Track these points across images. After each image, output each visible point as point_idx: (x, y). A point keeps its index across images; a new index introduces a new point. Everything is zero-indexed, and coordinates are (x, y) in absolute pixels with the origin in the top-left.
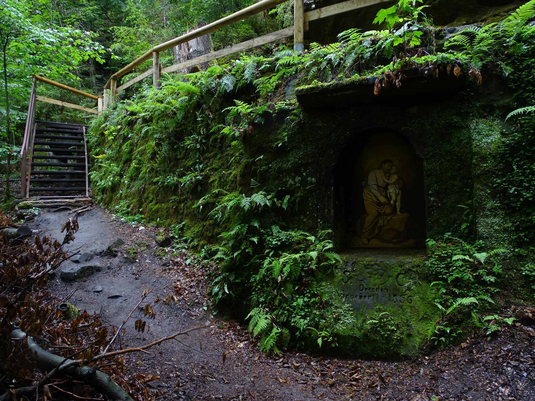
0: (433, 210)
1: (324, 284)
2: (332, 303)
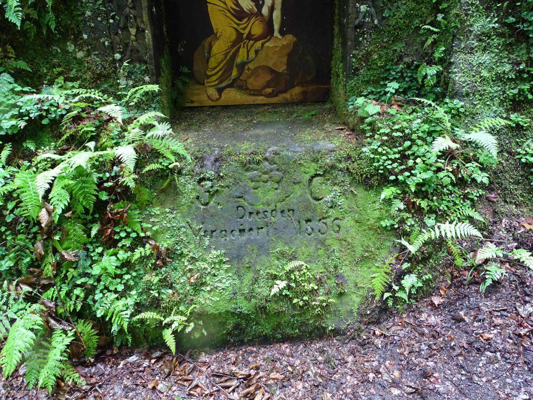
0: (363, 33)
1: (156, 210)
2: (182, 253)
